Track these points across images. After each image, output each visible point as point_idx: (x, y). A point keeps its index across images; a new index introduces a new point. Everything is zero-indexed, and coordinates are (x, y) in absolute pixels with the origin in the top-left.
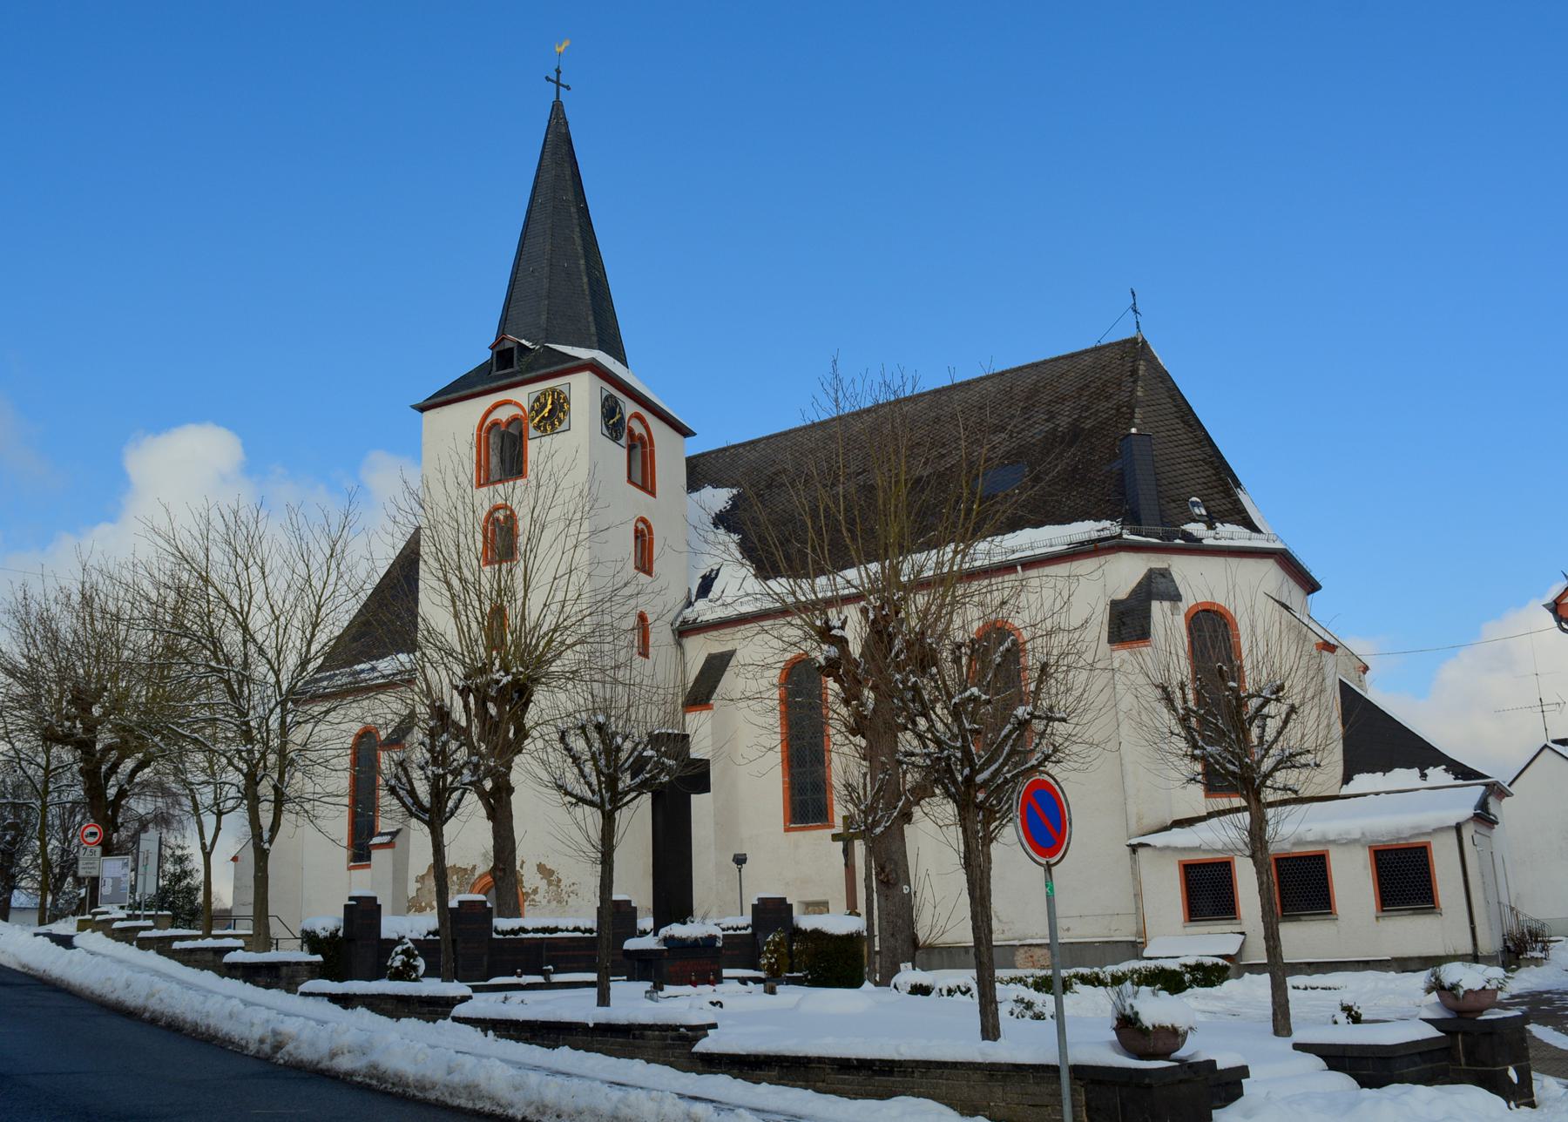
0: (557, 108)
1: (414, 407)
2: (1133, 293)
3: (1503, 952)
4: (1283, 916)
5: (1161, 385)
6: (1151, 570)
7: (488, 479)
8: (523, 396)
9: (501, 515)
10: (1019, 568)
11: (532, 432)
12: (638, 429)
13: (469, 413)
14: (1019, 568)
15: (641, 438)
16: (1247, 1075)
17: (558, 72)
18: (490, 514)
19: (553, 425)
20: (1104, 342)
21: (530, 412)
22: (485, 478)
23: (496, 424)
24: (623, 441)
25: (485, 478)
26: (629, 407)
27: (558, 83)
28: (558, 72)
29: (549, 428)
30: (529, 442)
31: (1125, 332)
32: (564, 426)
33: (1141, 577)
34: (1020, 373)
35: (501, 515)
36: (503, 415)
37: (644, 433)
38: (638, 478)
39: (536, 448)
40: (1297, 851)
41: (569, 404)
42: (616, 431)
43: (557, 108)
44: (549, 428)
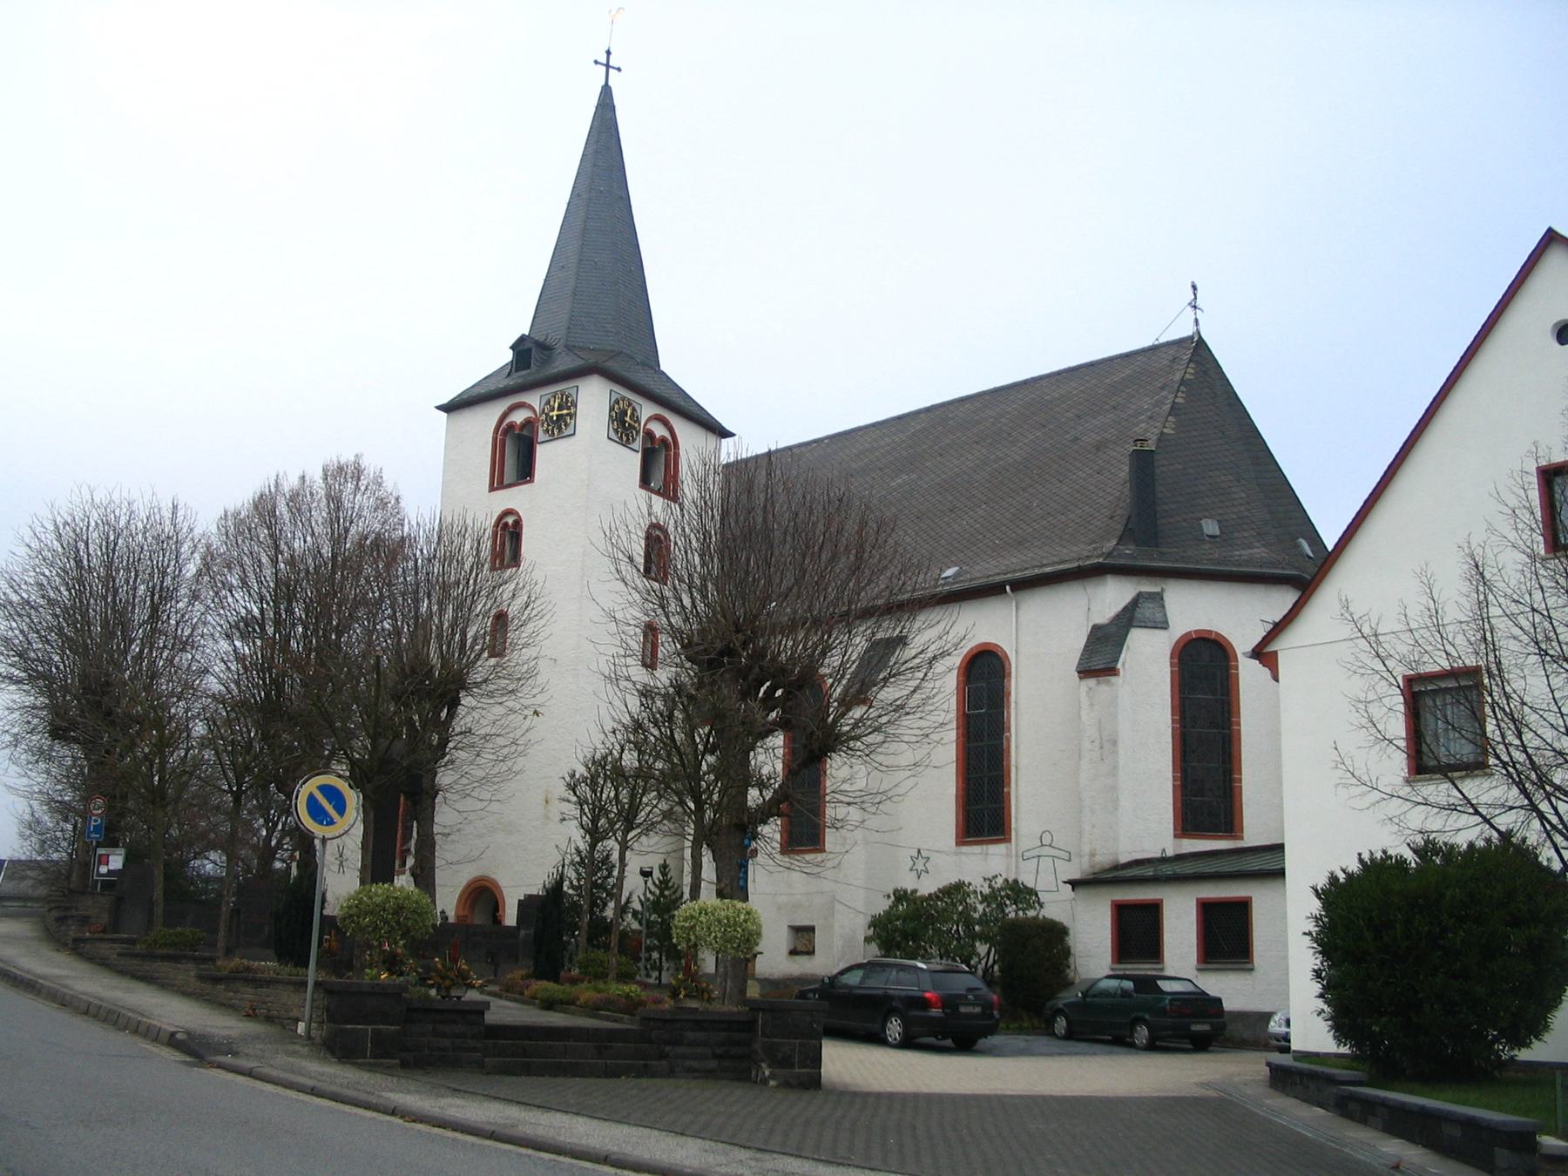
0: (606, 92)
1: (439, 408)
2: (1194, 287)
3: (797, 939)
4: (44, 842)
5: (1207, 390)
6: (1140, 595)
7: (502, 483)
8: (535, 399)
9: (510, 520)
10: (1008, 588)
11: (541, 436)
12: (659, 431)
13: (485, 421)
14: (1008, 588)
15: (663, 440)
16: (489, 1008)
17: (608, 53)
18: (501, 518)
19: (560, 430)
20: (1163, 340)
21: (541, 415)
22: (498, 482)
23: (511, 426)
24: (638, 444)
25: (498, 482)
26: (647, 410)
27: (608, 66)
28: (608, 53)
29: (556, 432)
30: (538, 446)
31: (1184, 330)
32: (570, 431)
33: (1128, 601)
34: (1059, 377)
35: (510, 520)
36: (519, 417)
37: (667, 435)
38: (657, 481)
39: (545, 454)
40: (1228, 895)
41: (576, 407)
42: (627, 435)
43: (606, 92)
44: (556, 432)
